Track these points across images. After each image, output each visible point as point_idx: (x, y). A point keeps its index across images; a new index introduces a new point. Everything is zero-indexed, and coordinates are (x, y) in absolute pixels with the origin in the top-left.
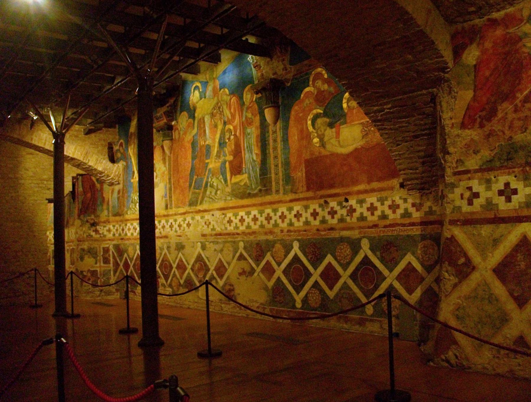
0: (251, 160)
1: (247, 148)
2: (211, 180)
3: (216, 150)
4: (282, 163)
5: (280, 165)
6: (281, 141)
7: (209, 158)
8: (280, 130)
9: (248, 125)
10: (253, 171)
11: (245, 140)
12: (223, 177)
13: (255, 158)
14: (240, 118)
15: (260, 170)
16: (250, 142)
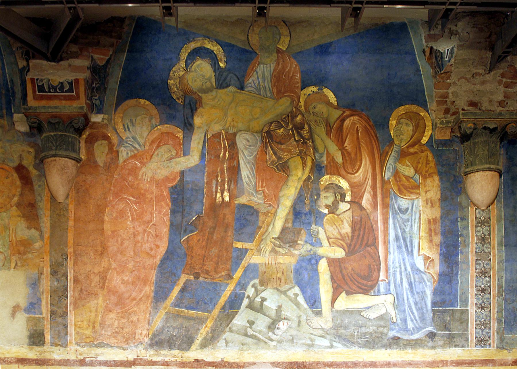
0: (409, 269)
1: (397, 238)
2: (257, 293)
3: (279, 224)
4: (500, 286)
5: (494, 291)
6: (500, 244)
7: (251, 238)
8: (499, 221)
9: (399, 190)
10: (412, 292)
11: (391, 221)
12: (303, 292)
13: (420, 263)
14: (374, 169)
15: (435, 292)
16: (407, 230)
